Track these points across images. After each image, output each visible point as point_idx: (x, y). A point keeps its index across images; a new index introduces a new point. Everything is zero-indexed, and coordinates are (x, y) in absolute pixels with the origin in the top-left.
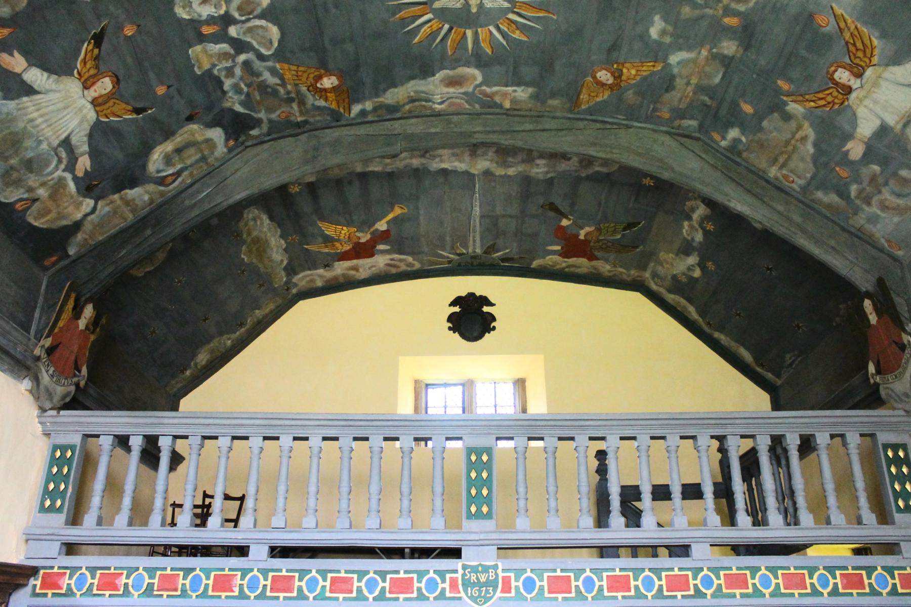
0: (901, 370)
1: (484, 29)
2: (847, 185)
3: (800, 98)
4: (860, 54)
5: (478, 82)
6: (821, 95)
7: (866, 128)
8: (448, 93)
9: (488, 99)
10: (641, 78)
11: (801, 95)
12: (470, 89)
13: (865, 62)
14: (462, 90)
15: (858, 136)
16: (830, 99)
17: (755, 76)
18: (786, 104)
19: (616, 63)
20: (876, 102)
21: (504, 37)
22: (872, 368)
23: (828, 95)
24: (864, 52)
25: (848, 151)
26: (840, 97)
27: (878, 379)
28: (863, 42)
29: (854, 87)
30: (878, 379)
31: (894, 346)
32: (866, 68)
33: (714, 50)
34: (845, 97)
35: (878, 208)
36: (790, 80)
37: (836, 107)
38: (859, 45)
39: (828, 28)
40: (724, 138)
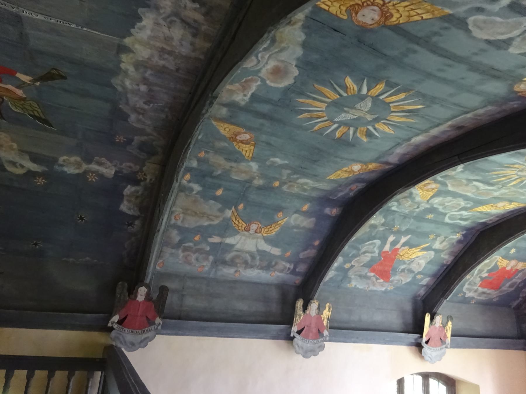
0: (140, 331)
1: (325, 106)
2: (191, 242)
3: (236, 214)
4: (266, 230)
5: (268, 82)
6: (241, 221)
7: (229, 240)
8: (267, 63)
9: (244, 81)
10: (240, 151)
11: (238, 214)
12: (261, 75)
13: (264, 232)
14: (264, 71)
15: (224, 239)
16: (240, 225)
17: (242, 194)
18: (230, 209)
19: (255, 143)
20: (245, 240)
21: (309, 110)
22: (116, 318)
23: (242, 224)
24: (268, 231)
25: (213, 237)
26: (243, 228)
27: (116, 326)
28: (272, 230)
29: (250, 232)
30: (116, 326)
31: (145, 318)
32: (261, 233)
33: (257, 178)
34: (243, 230)
35: (183, 255)
36: (245, 209)
37: (237, 228)
38: (271, 229)
39: (277, 218)
40: (189, 182)
